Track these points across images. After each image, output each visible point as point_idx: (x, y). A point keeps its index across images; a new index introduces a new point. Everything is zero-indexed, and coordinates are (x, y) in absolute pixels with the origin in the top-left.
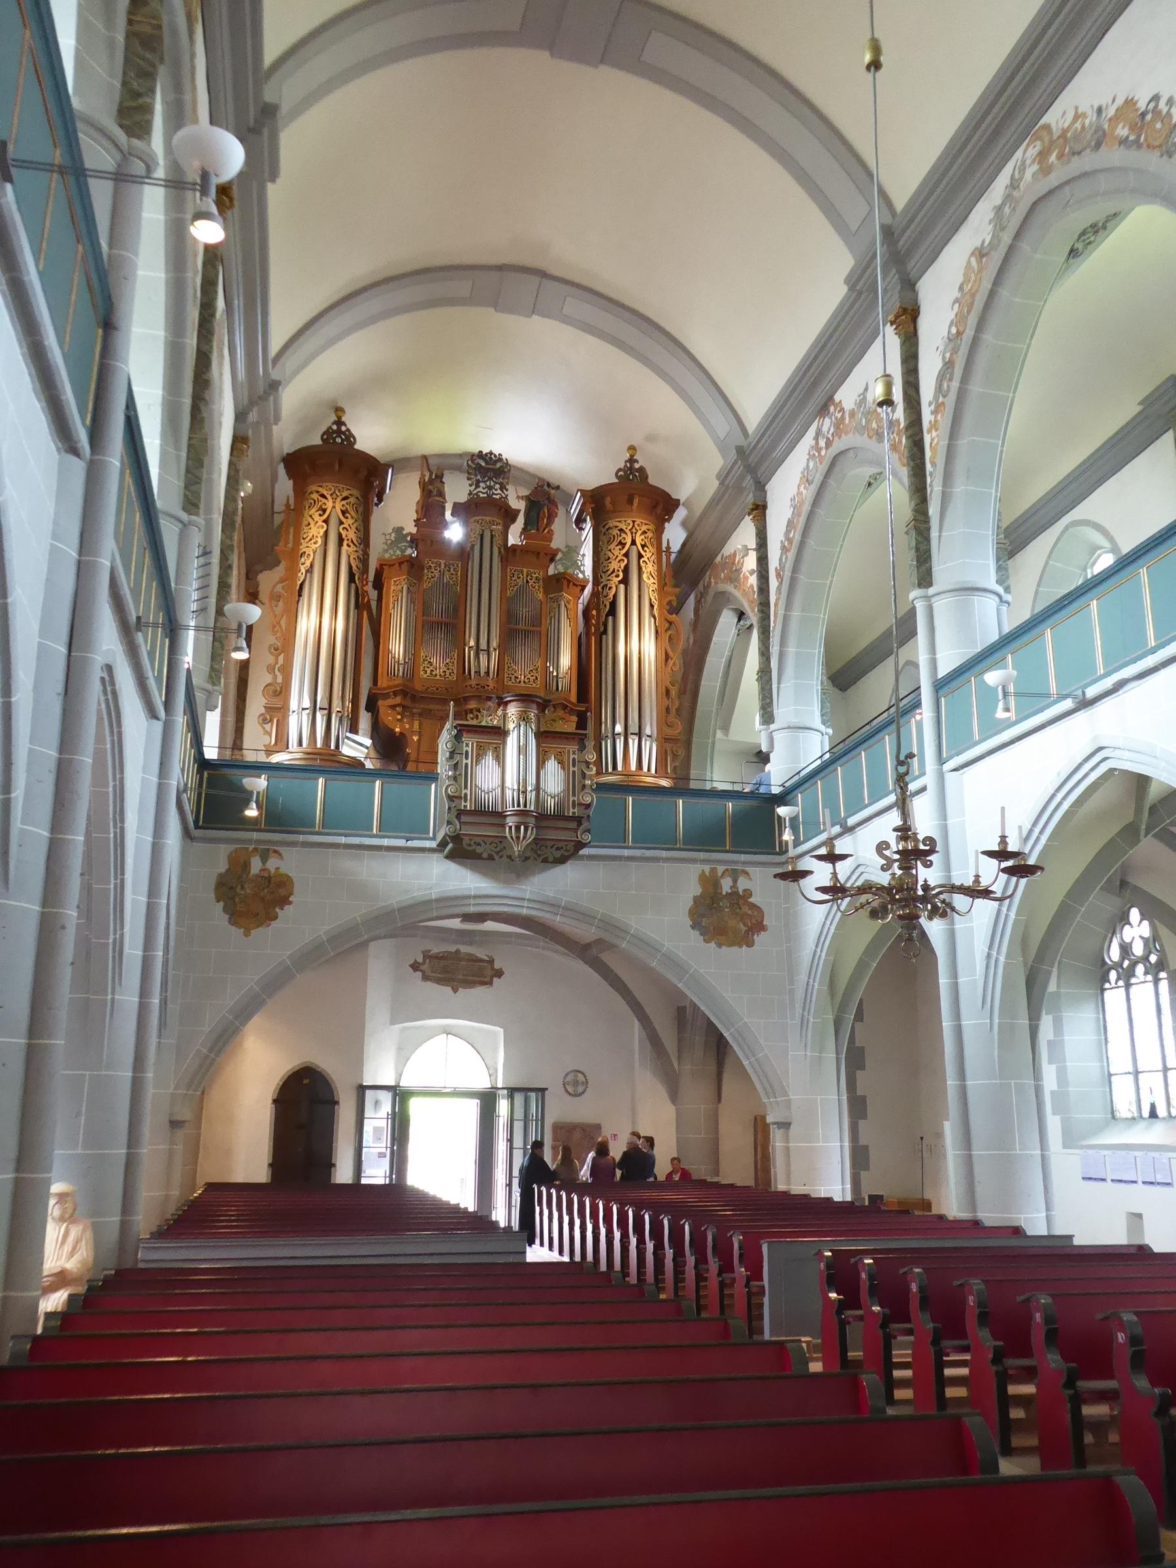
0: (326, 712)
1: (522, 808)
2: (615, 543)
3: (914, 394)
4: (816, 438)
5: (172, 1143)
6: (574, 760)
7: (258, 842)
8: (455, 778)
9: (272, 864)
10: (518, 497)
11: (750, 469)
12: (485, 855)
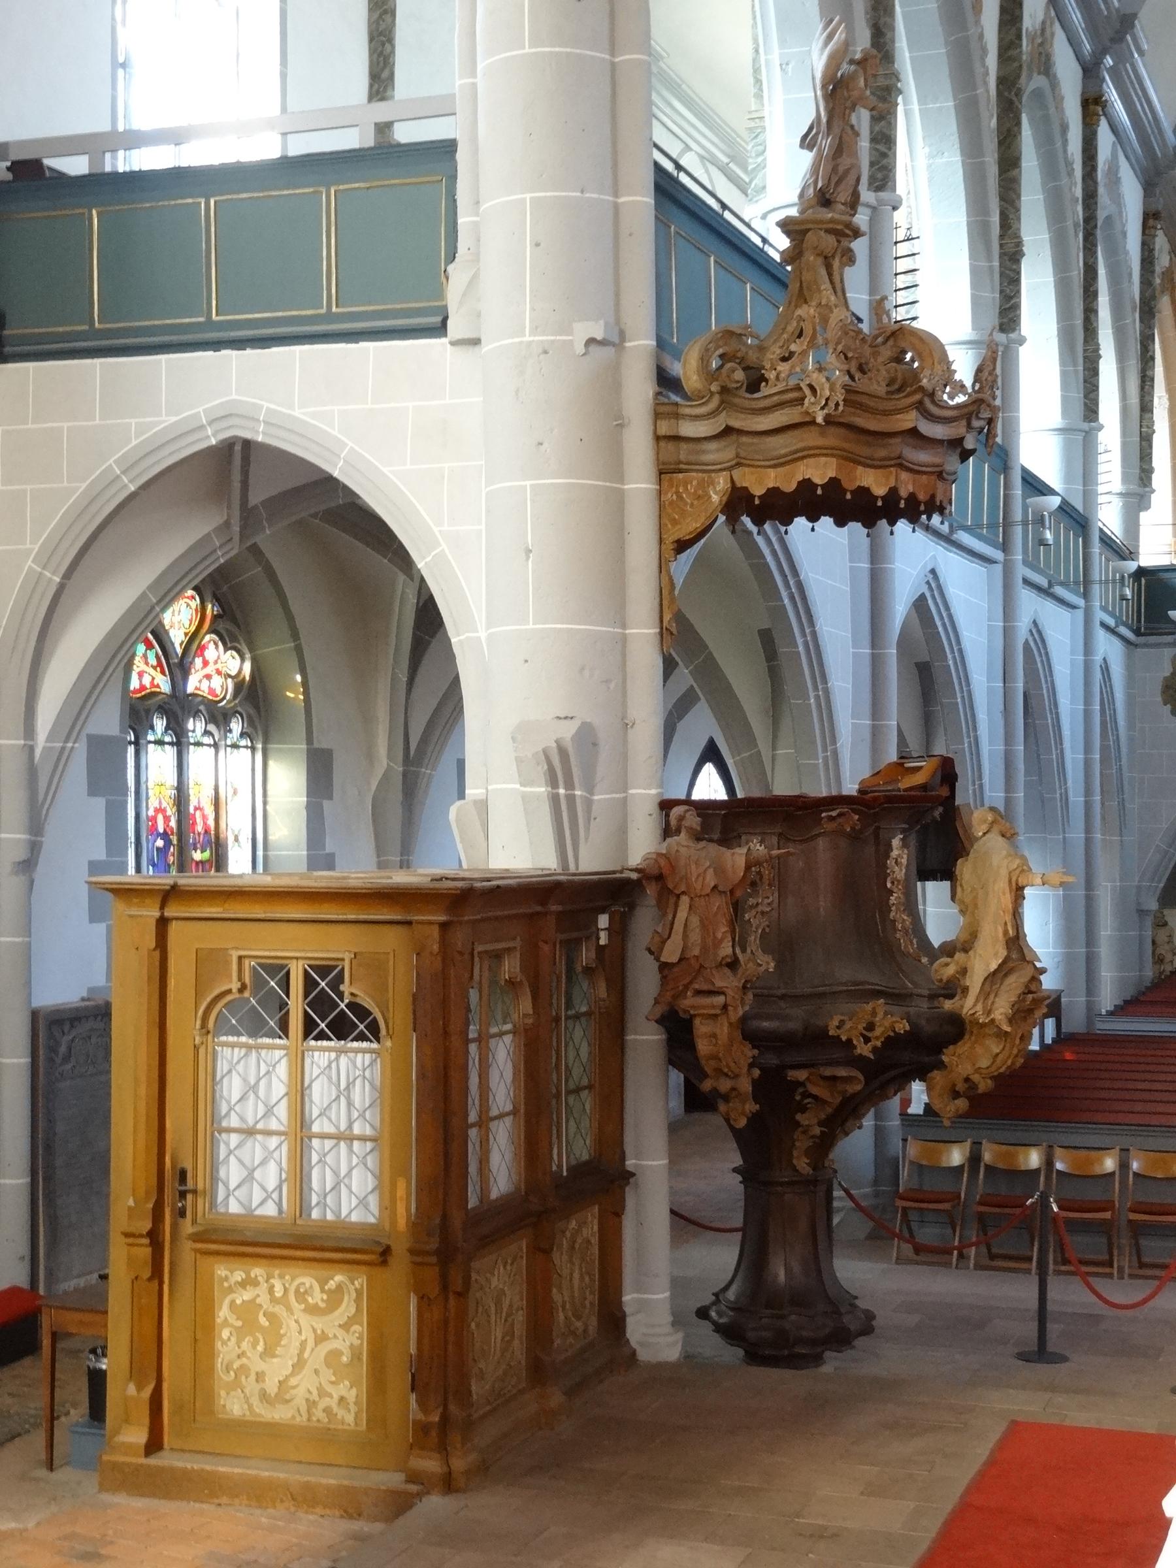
5: (1141, 929)
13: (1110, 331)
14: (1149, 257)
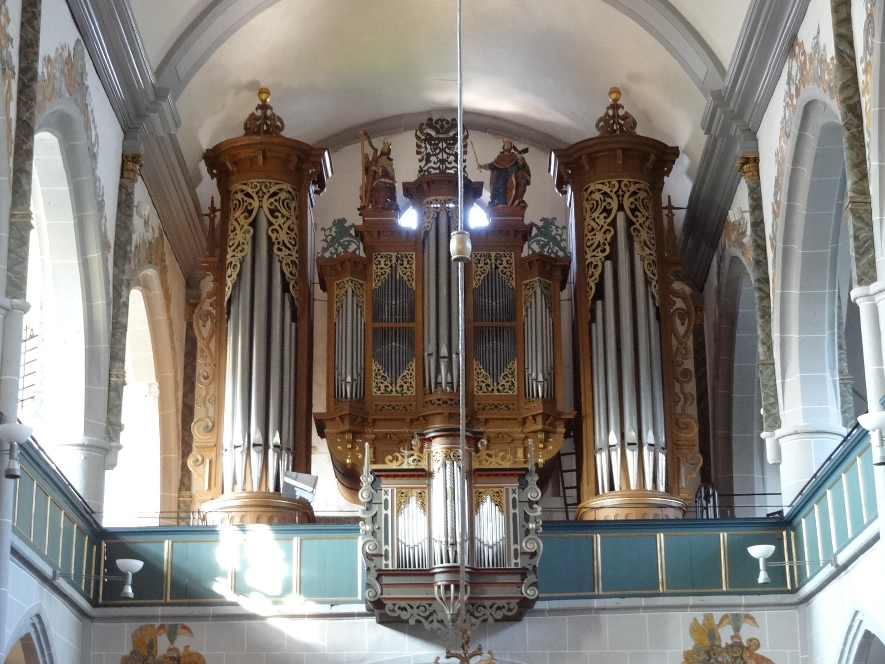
0: (261, 448)
1: (452, 564)
2: (599, 210)
3: (848, 51)
4: (788, 83)
6: (514, 499)
7: (164, 617)
8: (373, 533)
9: (181, 642)
10: (480, 167)
11: (733, 118)
12: (412, 622)
13: (76, 261)
14: (126, 200)
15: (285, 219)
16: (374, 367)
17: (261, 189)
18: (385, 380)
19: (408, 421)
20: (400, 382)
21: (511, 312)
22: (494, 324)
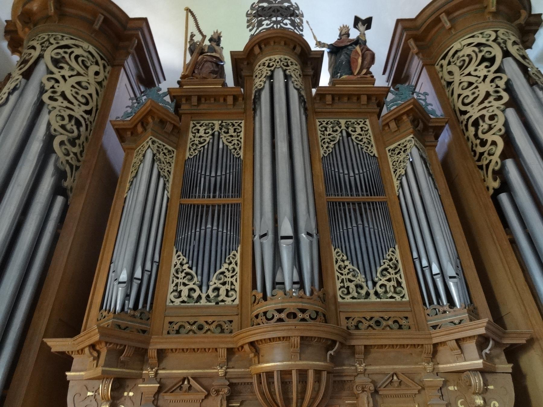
15: (74, 73)
16: (175, 260)
17: (48, 40)
18: (191, 279)
19: (223, 353)
20: (214, 282)
21: (376, 184)
22: (355, 198)
